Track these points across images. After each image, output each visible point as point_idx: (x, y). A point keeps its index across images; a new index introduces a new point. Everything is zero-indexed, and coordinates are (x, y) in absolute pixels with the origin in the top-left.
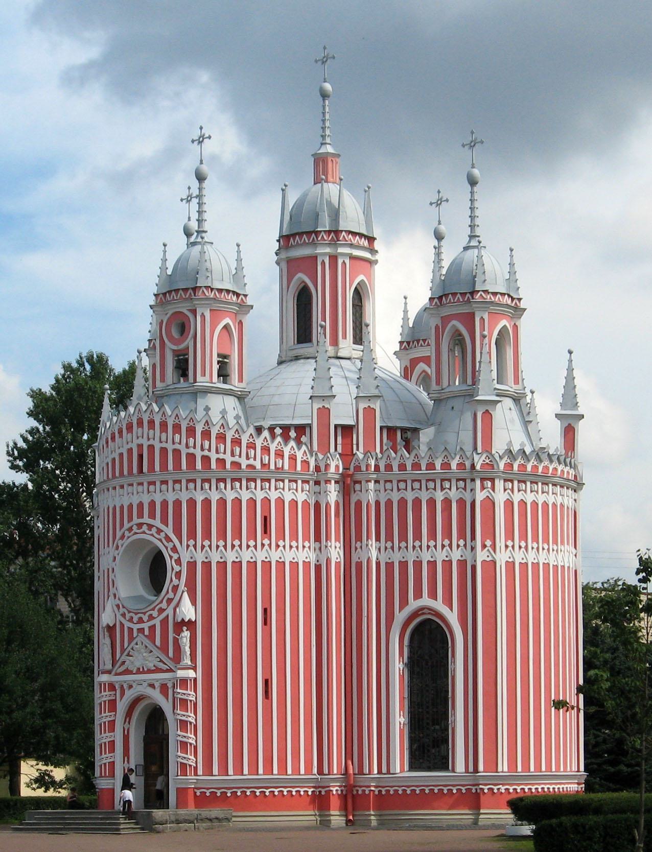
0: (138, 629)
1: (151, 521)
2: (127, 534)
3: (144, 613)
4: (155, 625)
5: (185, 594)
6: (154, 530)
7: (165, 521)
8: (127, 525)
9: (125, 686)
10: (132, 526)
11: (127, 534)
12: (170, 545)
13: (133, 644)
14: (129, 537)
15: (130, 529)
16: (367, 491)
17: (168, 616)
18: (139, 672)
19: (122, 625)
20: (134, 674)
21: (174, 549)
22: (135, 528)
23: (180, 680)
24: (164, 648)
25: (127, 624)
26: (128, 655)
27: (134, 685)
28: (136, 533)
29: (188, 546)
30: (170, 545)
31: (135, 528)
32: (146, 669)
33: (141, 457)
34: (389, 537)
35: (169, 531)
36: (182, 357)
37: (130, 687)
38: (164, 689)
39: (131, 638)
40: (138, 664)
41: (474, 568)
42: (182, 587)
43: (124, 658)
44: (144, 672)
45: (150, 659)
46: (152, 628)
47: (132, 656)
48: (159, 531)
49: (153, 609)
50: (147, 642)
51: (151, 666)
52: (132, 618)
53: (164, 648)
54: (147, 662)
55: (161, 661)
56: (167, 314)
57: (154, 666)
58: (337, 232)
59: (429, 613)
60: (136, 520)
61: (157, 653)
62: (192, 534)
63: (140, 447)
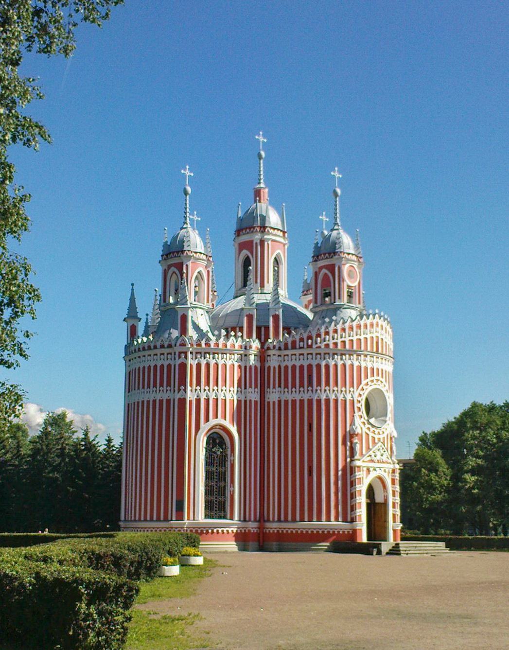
6: (383, 385)
8: (370, 379)
9: (371, 469)
18: (378, 462)
19: (367, 434)
25: (371, 435)
27: (377, 469)
39: (374, 443)
43: (371, 453)
52: (374, 431)
58: (265, 227)
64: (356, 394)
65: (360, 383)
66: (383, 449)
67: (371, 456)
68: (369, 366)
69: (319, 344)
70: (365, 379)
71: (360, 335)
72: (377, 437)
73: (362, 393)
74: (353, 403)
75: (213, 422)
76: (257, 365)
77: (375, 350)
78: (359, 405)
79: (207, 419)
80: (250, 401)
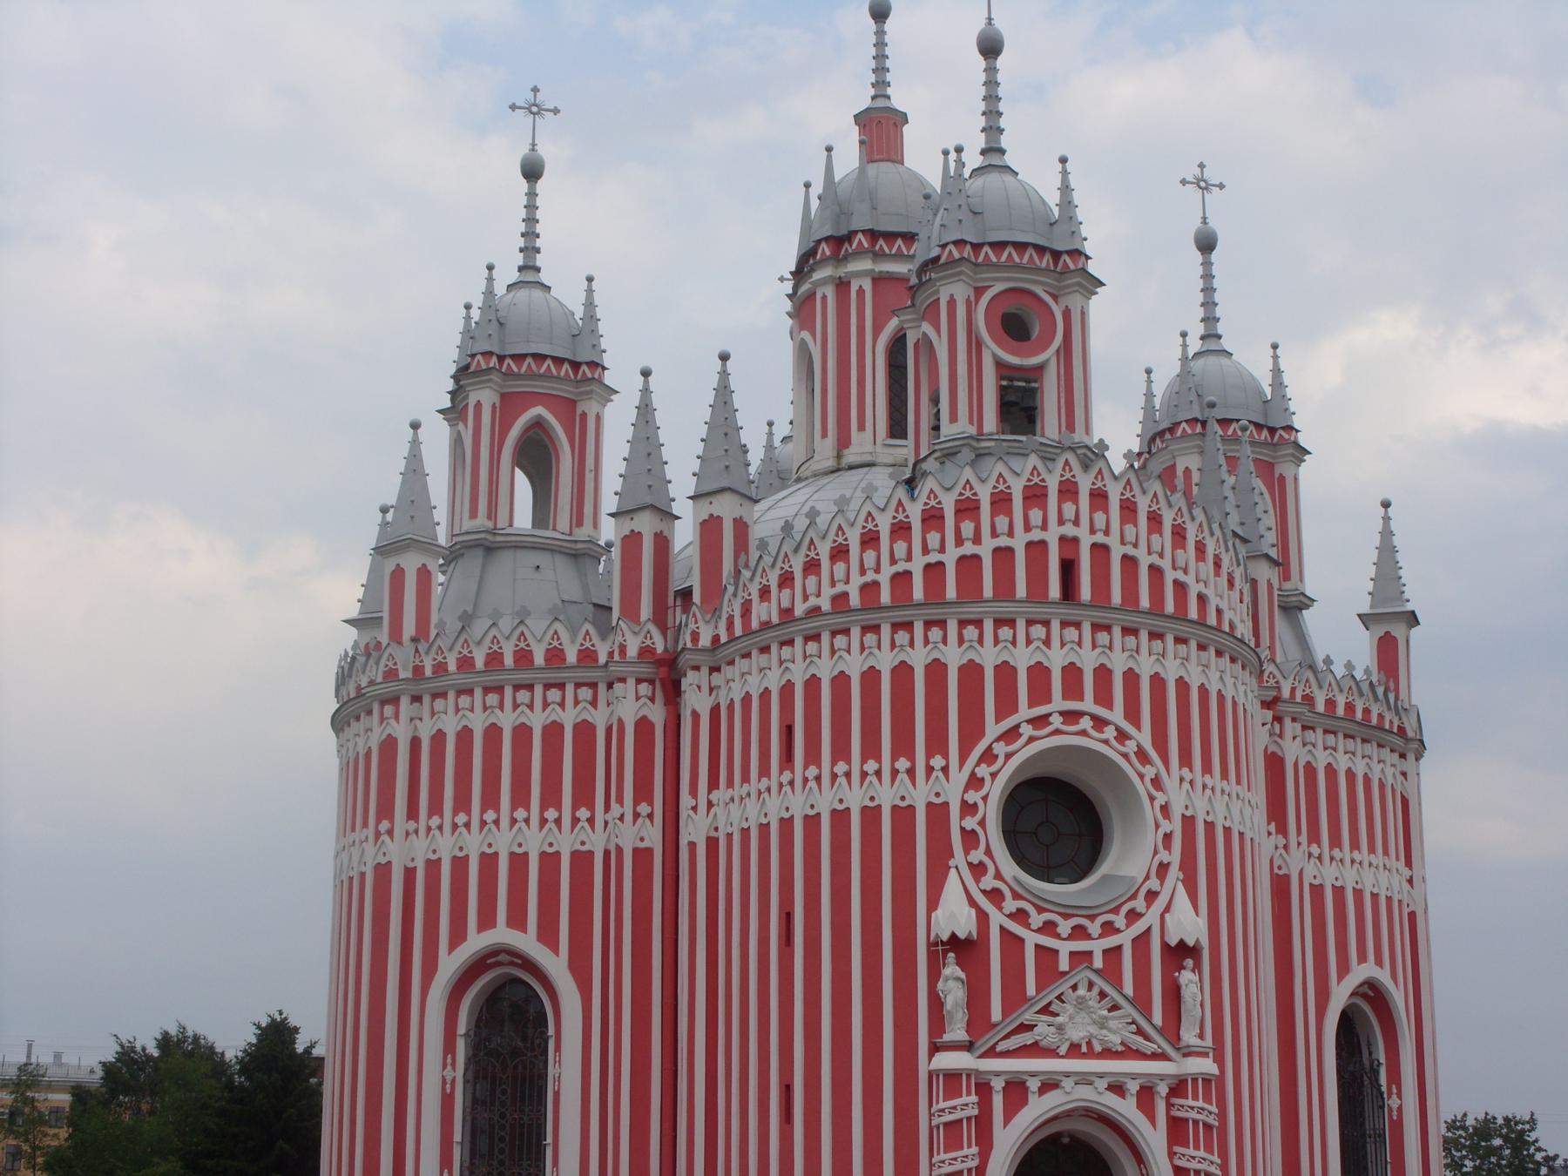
0: (1072, 954)
1: (1101, 712)
2: (1027, 730)
3: (1092, 918)
4: (1119, 948)
5: (1180, 886)
6: (1110, 733)
7: (1132, 714)
8: (1025, 712)
9: (1033, 1085)
10: (1050, 715)
11: (1027, 730)
12: (1149, 772)
13: (1064, 986)
14: (1031, 739)
15: (1040, 721)
16: (1294, 738)
17: (1149, 930)
18: (1074, 1051)
19: (1012, 943)
20: (1062, 1057)
21: (1157, 782)
22: (1057, 721)
23: (1192, 1079)
24: (1142, 1001)
25: (1031, 939)
26: (1045, 1010)
27: (1068, 1084)
28: (1057, 732)
29: (1182, 780)
30: (1149, 772)
31: (1057, 721)
32: (1098, 1048)
33: (1069, 569)
34: (1314, 837)
35: (1144, 737)
36: (1022, 384)
37: (1048, 1086)
38: (1146, 1096)
40: (1076, 1034)
41: (1412, 915)
42: (1174, 873)
43: (1028, 1016)
44: (1091, 1054)
45: (1112, 1024)
46: (1113, 954)
47: (1056, 1015)
48: (1122, 736)
49: (1115, 911)
50: (1100, 983)
51: (1115, 1040)
53: (1142, 1001)
54: (1104, 1032)
55: (1140, 1032)
56: (979, 292)
57: (1122, 1043)
59: (1365, 996)
60: (1058, 703)
61: (1128, 1009)
62: (1186, 760)
63: (1069, 543)
64: (959, 777)
65: (972, 729)
66: (1103, 995)
67: (1030, 1028)
68: (1022, 659)
69: (813, 601)
70: (998, 720)
71: (977, 540)
72: (1065, 948)
73: (983, 771)
74: (938, 813)
75: (476, 942)
76: (651, 717)
77: (1055, 591)
78: (970, 823)
79: (458, 936)
80: (619, 850)
